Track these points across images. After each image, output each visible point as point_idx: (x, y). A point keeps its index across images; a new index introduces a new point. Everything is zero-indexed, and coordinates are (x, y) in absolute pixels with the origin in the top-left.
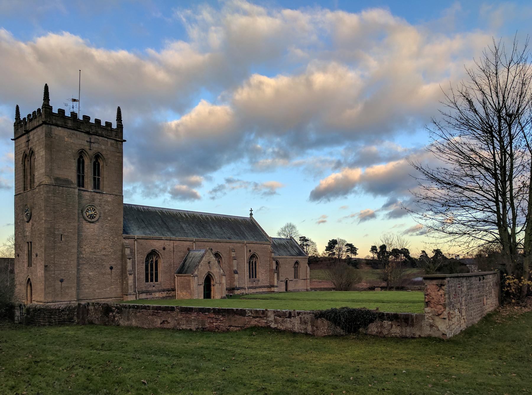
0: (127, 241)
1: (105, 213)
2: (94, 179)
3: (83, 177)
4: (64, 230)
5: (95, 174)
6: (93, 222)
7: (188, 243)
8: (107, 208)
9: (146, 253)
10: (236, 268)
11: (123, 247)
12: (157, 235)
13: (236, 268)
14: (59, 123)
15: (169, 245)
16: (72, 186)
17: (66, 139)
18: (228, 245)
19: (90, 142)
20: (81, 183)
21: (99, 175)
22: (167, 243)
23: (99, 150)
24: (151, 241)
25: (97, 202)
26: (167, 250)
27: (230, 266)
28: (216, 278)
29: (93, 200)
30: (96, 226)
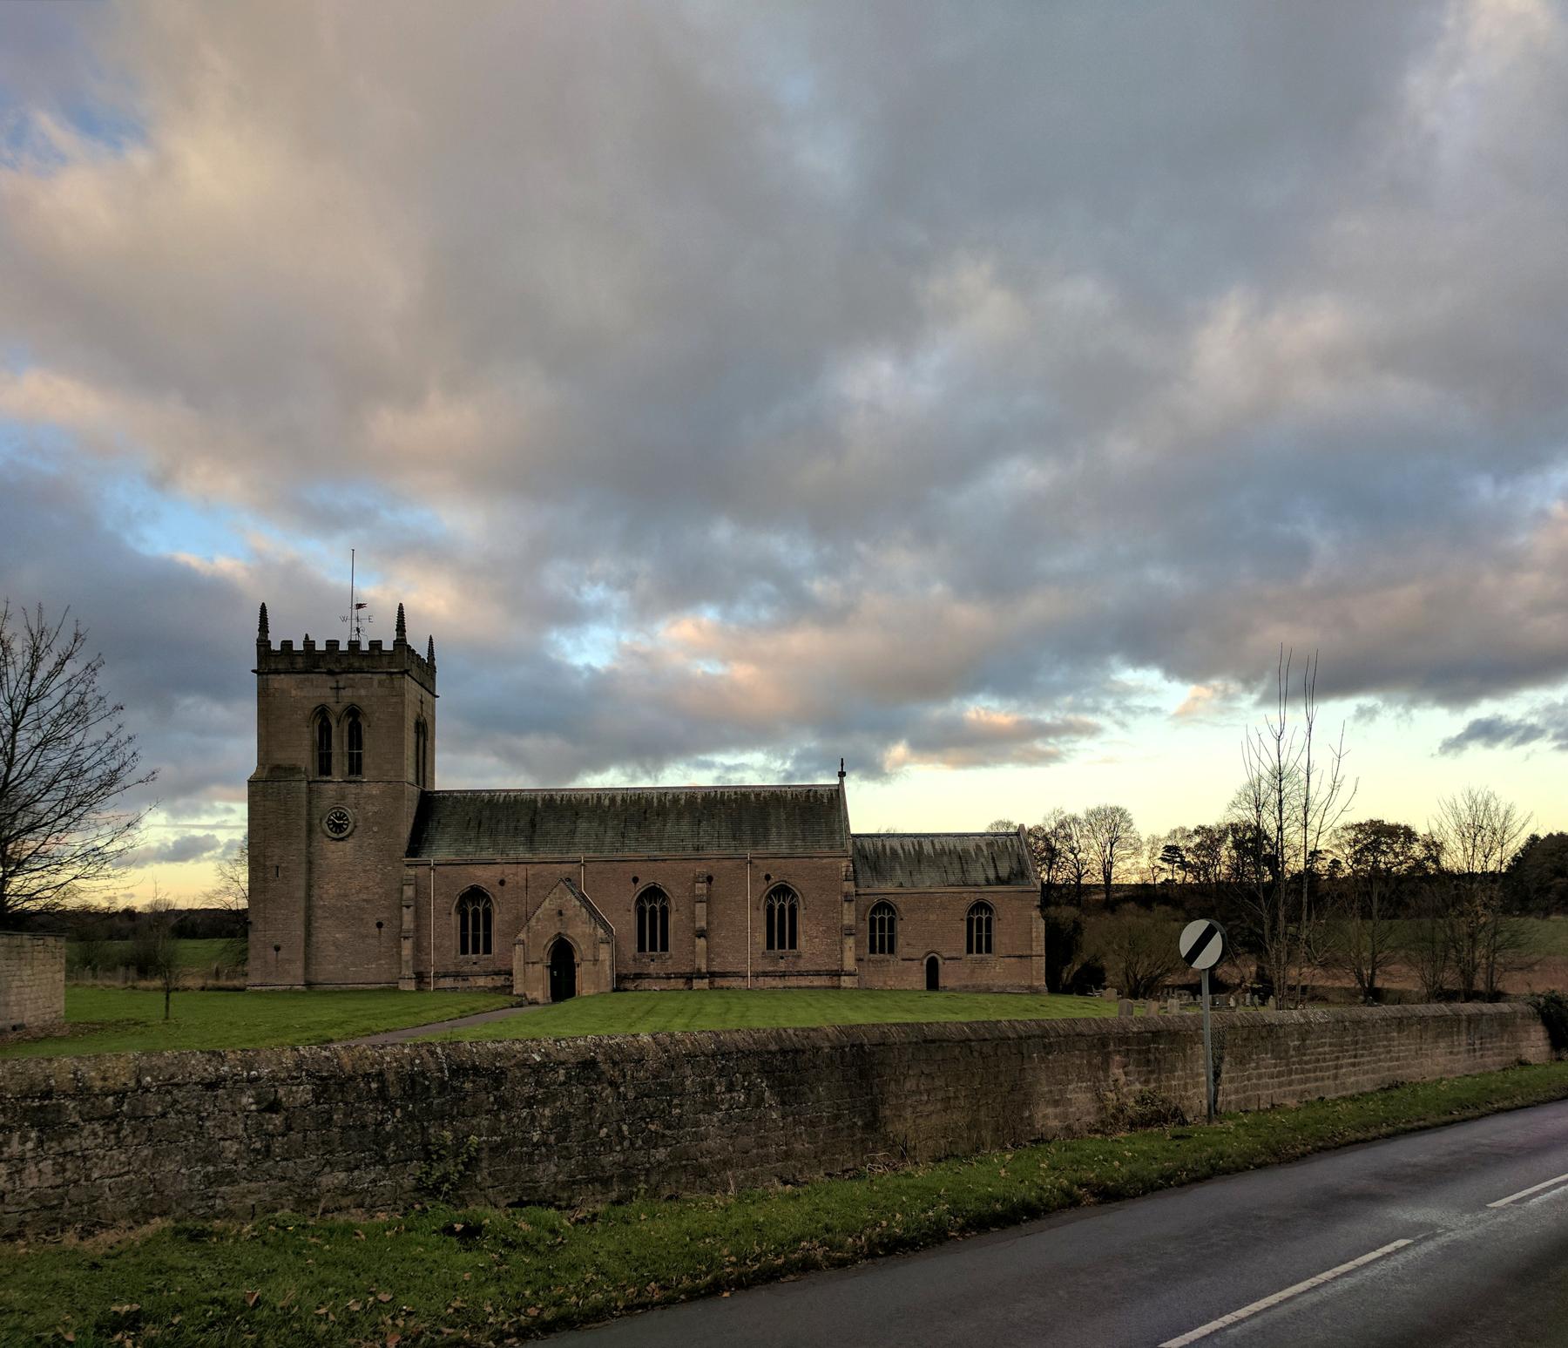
0: (412, 872)
1: (366, 819)
2: (351, 755)
3: (329, 756)
4: (281, 858)
5: (351, 747)
6: (342, 839)
7: (567, 868)
8: (371, 808)
9: (457, 893)
10: (703, 924)
11: (404, 882)
12: (486, 855)
13: (703, 924)
14: (280, 666)
15: (515, 874)
16: (297, 777)
17: (294, 693)
18: (692, 865)
19: (338, 688)
20: (325, 768)
21: (360, 748)
22: (509, 869)
23: (355, 701)
24: (471, 869)
25: (351, 799)
26: (508, 886)
27: (693, 919)
28: (582, 950)
29: (343, 798)
30: (348, 846)
